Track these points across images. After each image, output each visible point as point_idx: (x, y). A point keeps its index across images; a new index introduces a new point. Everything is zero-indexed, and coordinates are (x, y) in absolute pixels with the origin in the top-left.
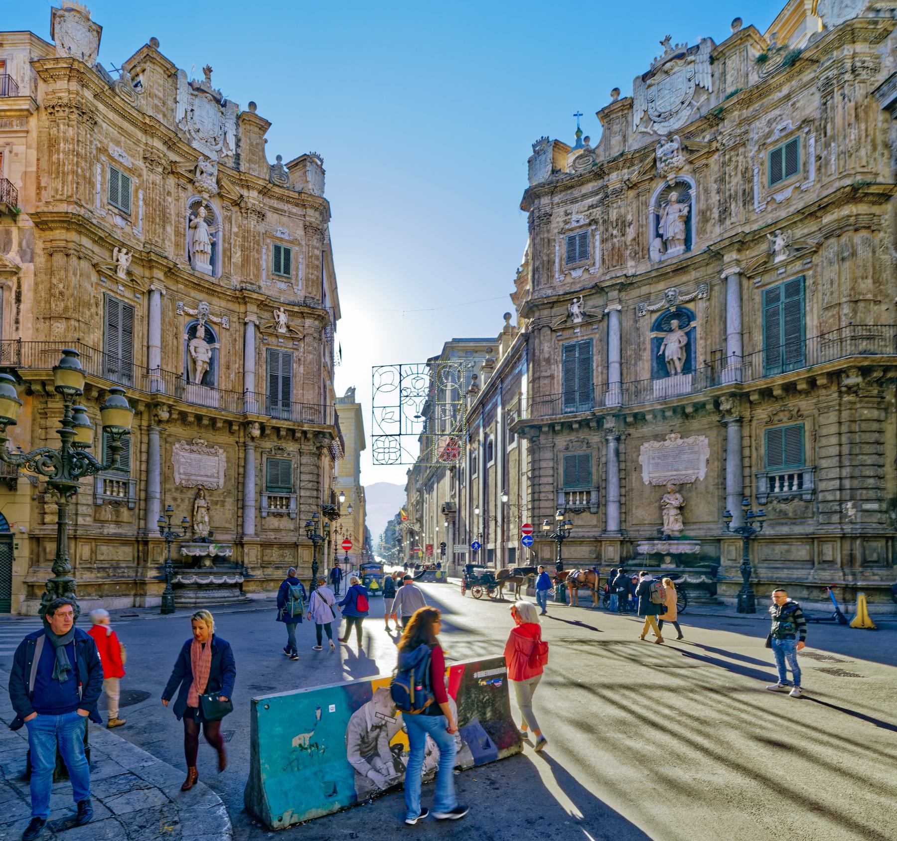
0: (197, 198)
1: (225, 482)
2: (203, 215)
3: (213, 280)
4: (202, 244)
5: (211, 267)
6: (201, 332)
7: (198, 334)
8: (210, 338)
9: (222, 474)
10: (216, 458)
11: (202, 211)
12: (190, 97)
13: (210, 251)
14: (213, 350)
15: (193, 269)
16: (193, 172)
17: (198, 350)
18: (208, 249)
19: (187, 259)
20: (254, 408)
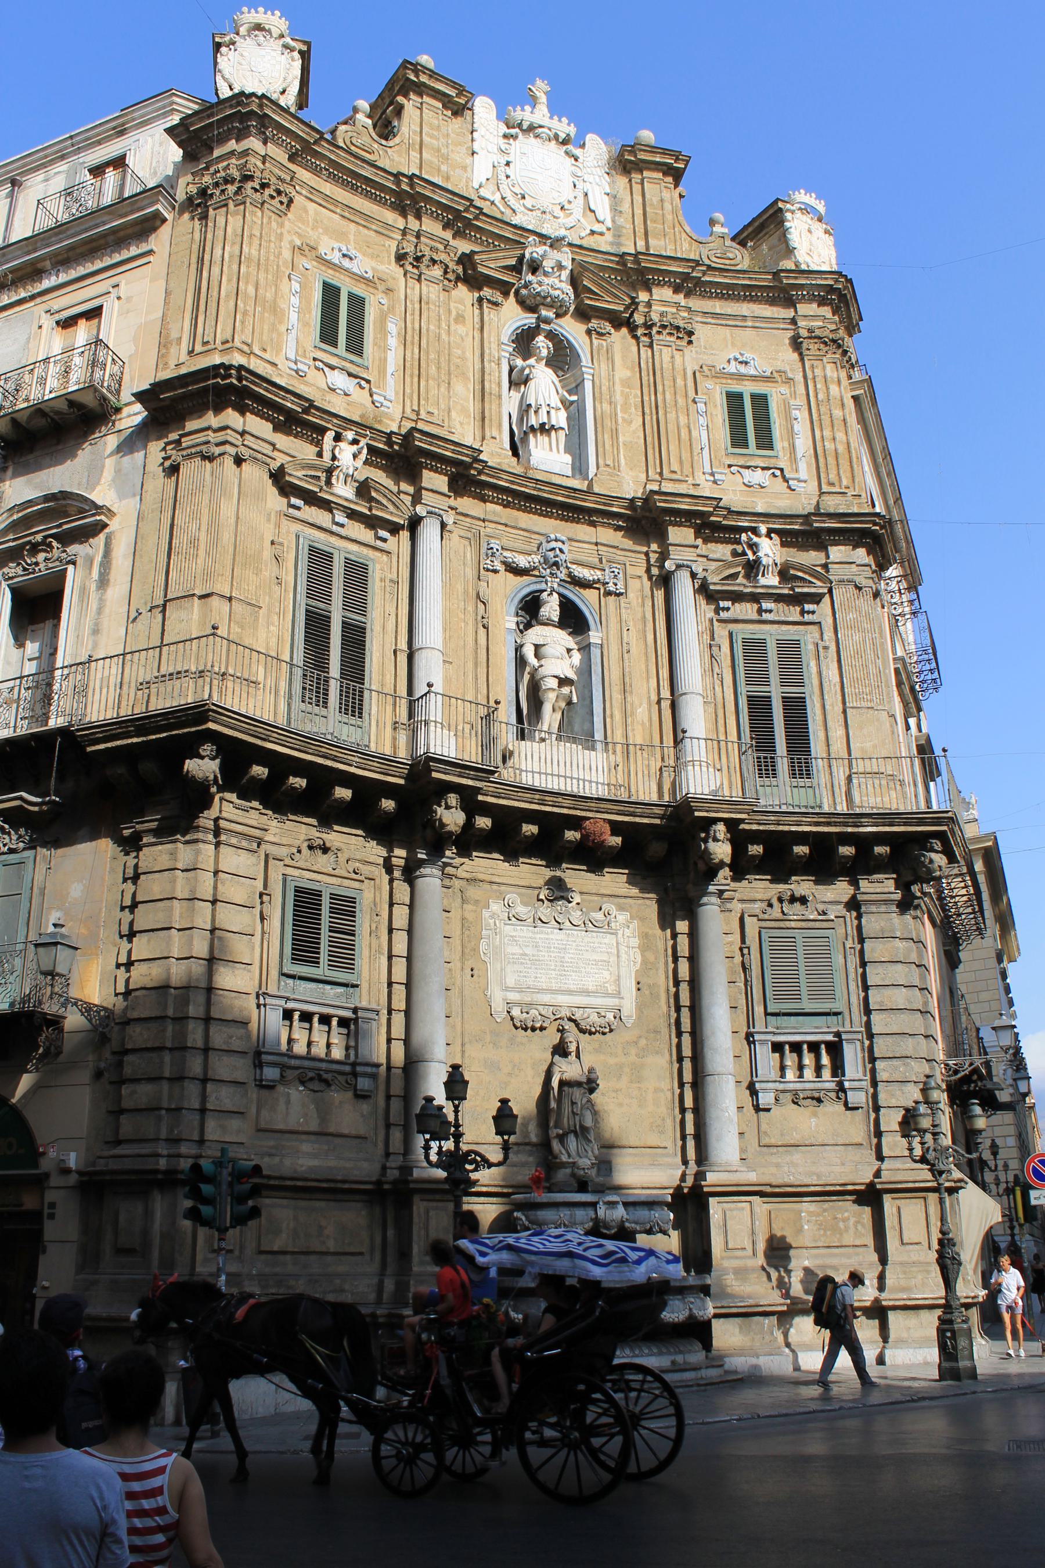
1: (640, 1007)
2: (544, 353)
4: (543, 411)
5: (568, 459)
6: (551, 608)
8: (573, 619)
10: (610, 939)
11: (541, 342)
12: (502, 141)
14: (585, 648)
15: (528, 467)
16: (517, 269)
17: (543, 650)
18: (560, 418)
19: (507, 446)
20: (706, 779)
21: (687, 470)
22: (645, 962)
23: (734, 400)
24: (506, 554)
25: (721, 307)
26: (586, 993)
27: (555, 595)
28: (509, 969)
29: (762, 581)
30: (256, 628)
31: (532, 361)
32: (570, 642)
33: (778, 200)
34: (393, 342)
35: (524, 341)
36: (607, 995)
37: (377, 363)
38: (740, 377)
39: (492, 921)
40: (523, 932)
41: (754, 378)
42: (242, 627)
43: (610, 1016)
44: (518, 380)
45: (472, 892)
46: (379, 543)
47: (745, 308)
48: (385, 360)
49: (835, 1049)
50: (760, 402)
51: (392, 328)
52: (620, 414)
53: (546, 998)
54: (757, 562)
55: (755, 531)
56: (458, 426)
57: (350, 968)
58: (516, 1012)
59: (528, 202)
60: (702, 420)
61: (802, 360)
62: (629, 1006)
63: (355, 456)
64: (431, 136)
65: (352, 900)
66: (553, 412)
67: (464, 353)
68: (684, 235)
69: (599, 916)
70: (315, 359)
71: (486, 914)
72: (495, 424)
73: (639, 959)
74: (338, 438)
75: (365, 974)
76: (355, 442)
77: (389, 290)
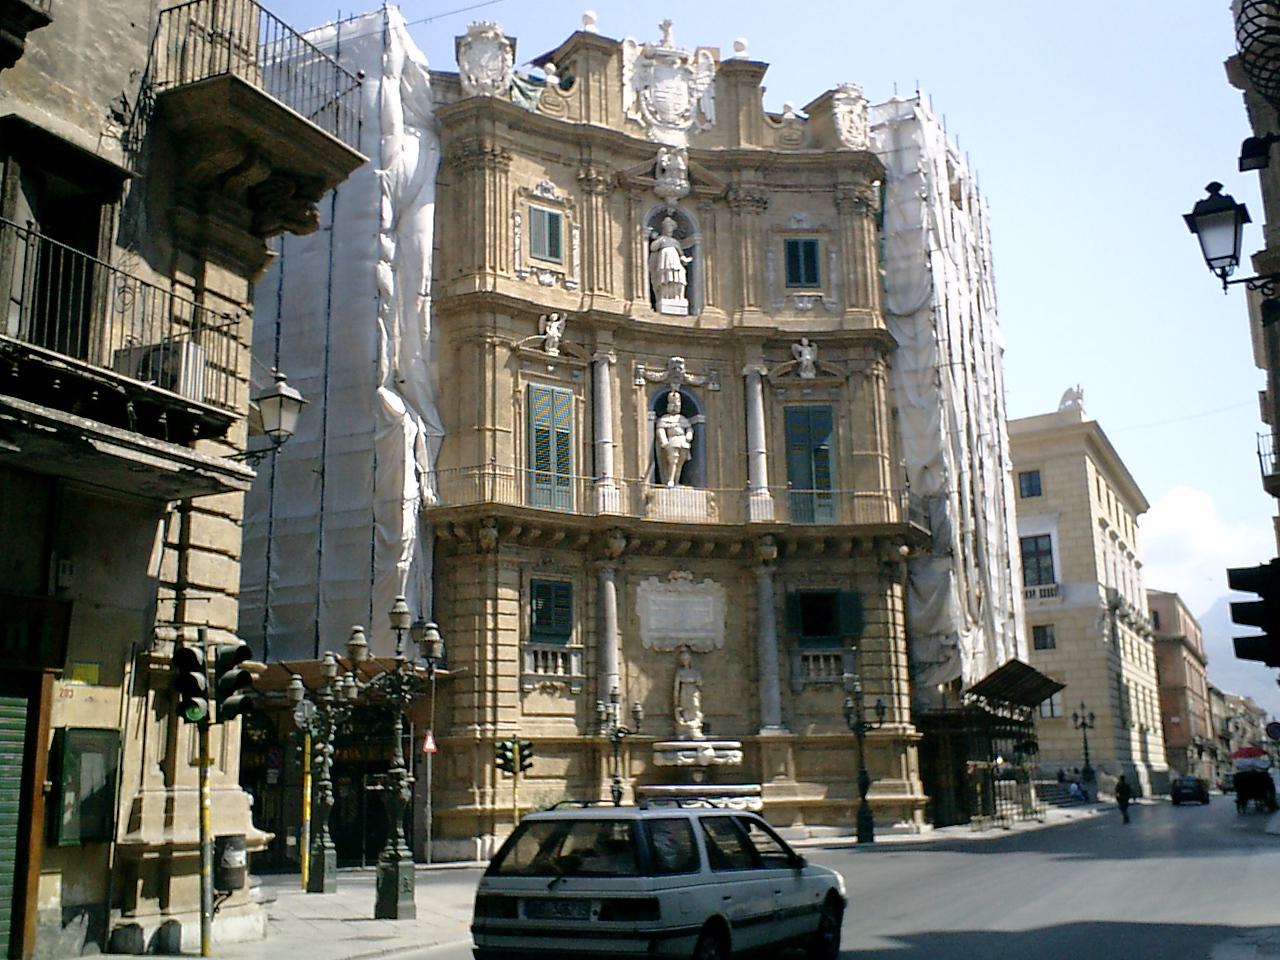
0: (660, 206)
3: (688, 322)
6: (676, 399)
7: (670, 407)
8: (688, 410)
11: (670, 224)
13: (683, 281)
18: (681, 277)
23: (792, 247)
24: (649, 373)
26: (694, 630)
29: (804, 375)
31: (663, 239)
32: (686, 422)
34: (576, 242)
35: (657, 223)
36: (707, 631)
38: (797, 231)
40: (659, 598)
41: (807, 231)
44: (655, 253)
46: (574, 379)
47: (802, 179)
50: (811, 247)
51: (576, 233)
53: (673, 635)
54: (799, 364)
58: (655, 643)
60: (771, 264)
62: (719, 636)
69: (702, 585)
73: (726, 609)
74: (548, 319)
76: (558, 320)
77: (572, 207)
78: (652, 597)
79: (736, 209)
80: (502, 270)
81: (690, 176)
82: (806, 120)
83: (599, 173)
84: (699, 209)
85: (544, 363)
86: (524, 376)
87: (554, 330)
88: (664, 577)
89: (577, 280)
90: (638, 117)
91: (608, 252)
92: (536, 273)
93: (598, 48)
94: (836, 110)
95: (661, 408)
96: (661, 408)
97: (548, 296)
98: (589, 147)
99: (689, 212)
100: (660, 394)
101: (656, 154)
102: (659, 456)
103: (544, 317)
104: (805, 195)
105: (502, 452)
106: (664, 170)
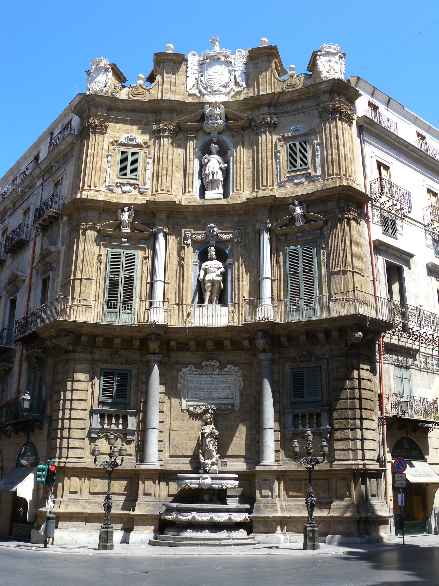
0: (208, 138)
1: (241, 403)
3: (224, 202)
8: (221, 256)
9: (239, 395)
18: (220, 176)
21: (270, 183)
22: (245, 385)
25: (290, 107)
26: (220, 399)
27: (213, 248)
28: (189, 392)
30: (91, 287)
32: (220, 264)
33: (314, 52)
34: (150, 166)
36: (228, 399)
37: (142, 176)
39: (183, 376)
42: (86, 287)
43: (230, 407)
45: (176, 366)
48: (146, 174)
49: (319, 415)
52: (245, 166)
55: (294, 204)
56: (176, 191)
57: (125, 397)
59: (209, 90)
61: (321, 121)
62: (237, 402)
63: (129, 216)
64: (167, 77)
65: (126, 374)
66: (215, 175)
67: (180, 160)
68: (275, 80)
70: (117, 183)
71: (181, 373)
72: (190, 186)
74: (123, 211)
75: (132, 399)
76: (129, 210)
77: (148, 147)
78: (190, 378)
79: (256, 132)
80: (95, 187)
81: (227, 118)
82: (311, 75)
83: (165, 125)
84: (233, 136)
85: (119, 238)
86: (105, 246)
87: (125, 217)
88: (198, 366)
89: (148, 186)
90: (196, 92)
91: (169, 168)
92: (120, 186)
93: (169, 61)
94: (317, 62)
95: (203, 257)
96: (203, 257)
97: (126, 199)
98: (161, 113)
99: (226, 139)
100: (203, 248)
101: (203, 108)
102: (200, 286)
103: (120, 210)
104: (301, 115)
105: (85, 291)
106: (208, 117)
